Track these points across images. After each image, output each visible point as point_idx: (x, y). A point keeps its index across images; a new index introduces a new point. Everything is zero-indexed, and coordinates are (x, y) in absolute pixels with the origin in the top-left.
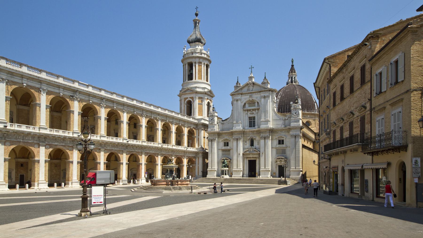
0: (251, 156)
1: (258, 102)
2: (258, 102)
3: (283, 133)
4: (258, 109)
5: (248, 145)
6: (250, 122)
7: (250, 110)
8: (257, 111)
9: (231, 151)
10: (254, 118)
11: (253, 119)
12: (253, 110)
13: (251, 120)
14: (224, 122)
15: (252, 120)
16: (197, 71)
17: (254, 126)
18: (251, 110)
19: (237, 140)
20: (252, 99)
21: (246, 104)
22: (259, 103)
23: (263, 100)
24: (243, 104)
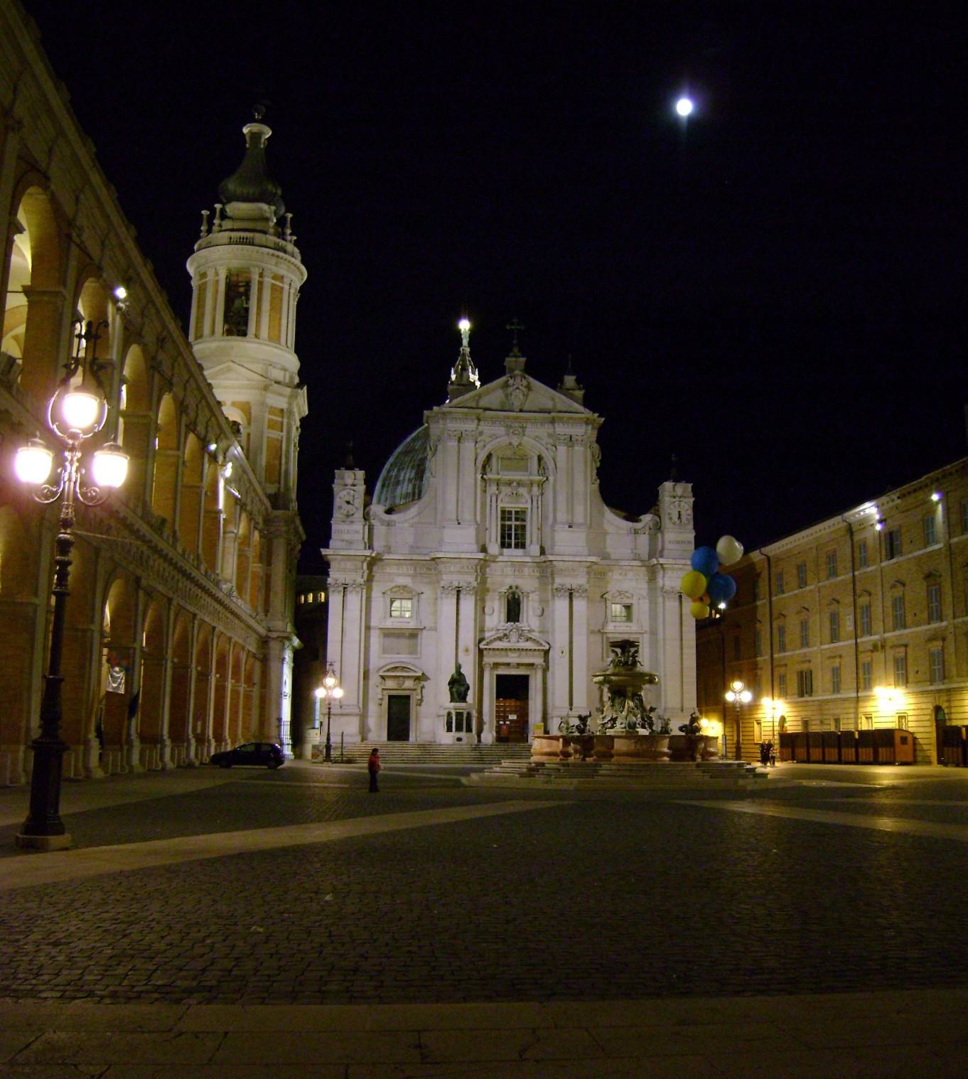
0: (513, 658)
1: (540, 458)
2: (540, 458)
3: (631, 580)
4: (541, 485)
5: (496, 614)
6: (503, 526)
7: (509, 483)
8: (535, 489)
9: (425, 637)
10: (520, 515)
11: (517, 519)
12: (519, 484)
13: (510, 519)
14: (393, 517)
15: (513, 523)
16: (266, 305)
17: (521, 545)
18: (515, 484)
19: (458, 592)
20: (520, 444)
21: (494, 460)
22: (545, 459)
23: (562, 449)
24: (482, 457)
